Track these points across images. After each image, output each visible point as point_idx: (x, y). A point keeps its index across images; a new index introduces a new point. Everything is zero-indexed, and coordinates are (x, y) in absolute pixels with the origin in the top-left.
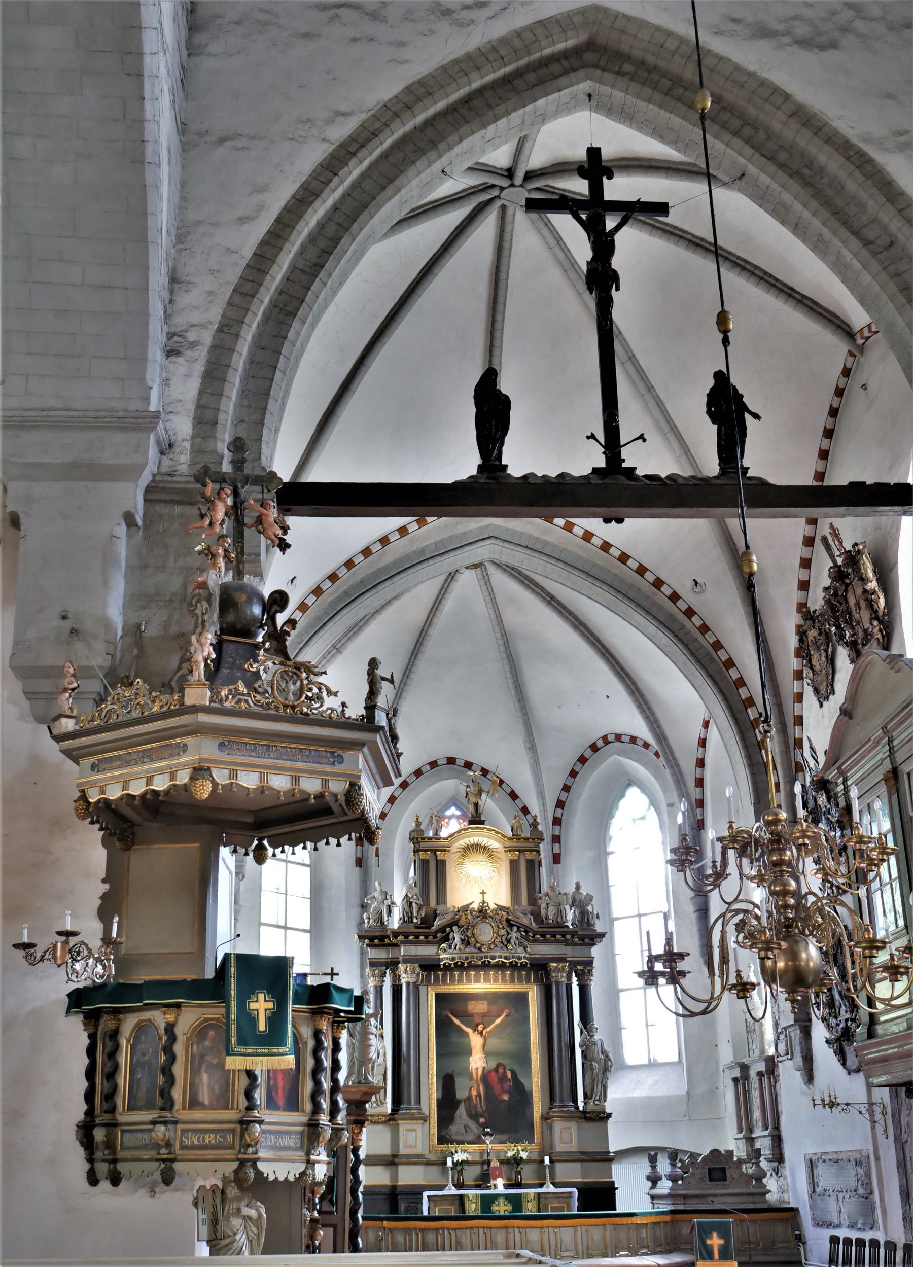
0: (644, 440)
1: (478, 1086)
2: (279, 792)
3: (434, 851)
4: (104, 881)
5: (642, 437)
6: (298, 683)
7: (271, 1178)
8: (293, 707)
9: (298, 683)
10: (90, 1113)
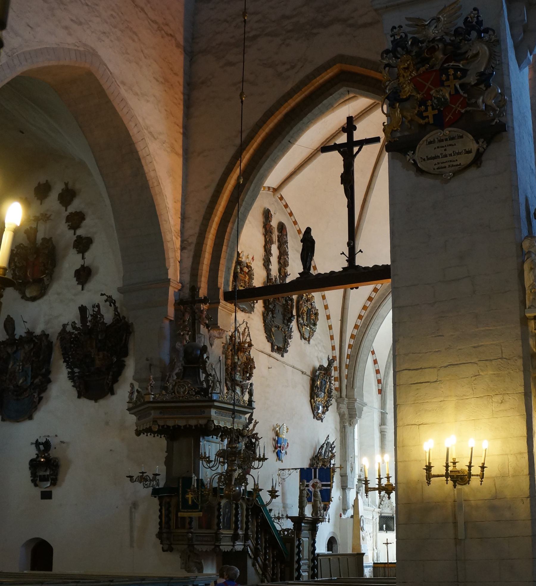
0: (362, 252)
2: (181, 426)
4: (166, 452)
5: (360, 251)
6: (184, 388)
7: (200, 550)
8: (183, 397)
9: (184, 388)
10: (160, 528)
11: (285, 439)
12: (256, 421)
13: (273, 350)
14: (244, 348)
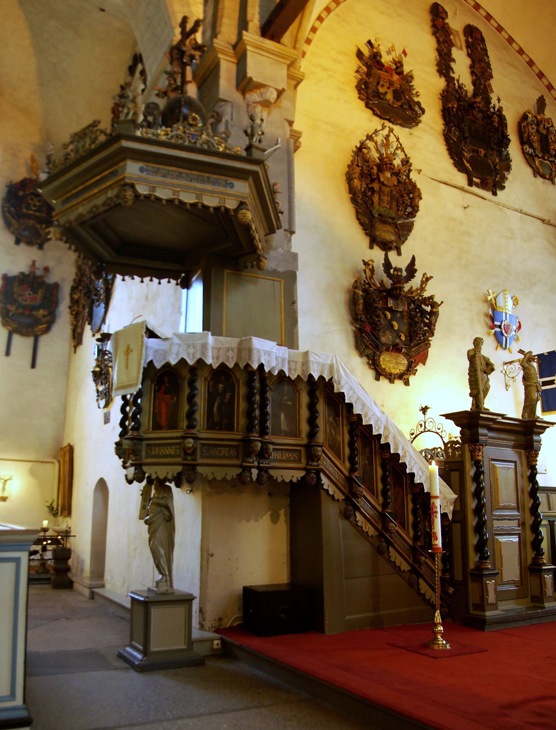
11: (510, 315)
12: (424, 274)
13: (471, 183)
14: (386, 164)
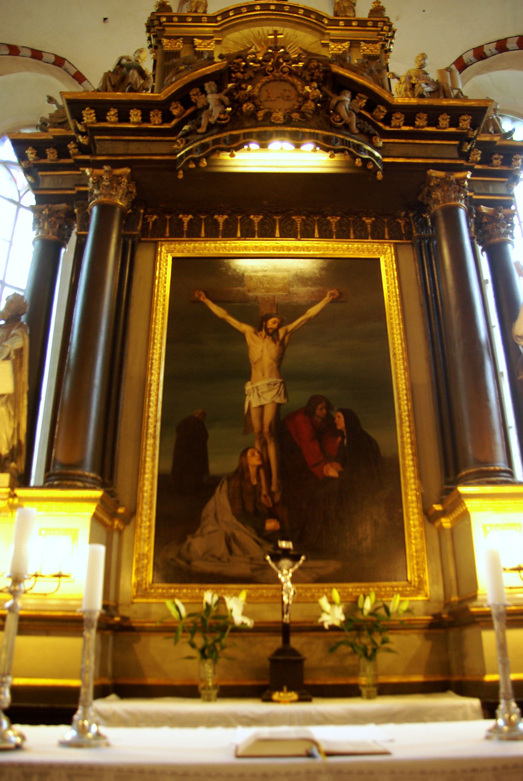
1: (264, 445)
3: (189, 40)
